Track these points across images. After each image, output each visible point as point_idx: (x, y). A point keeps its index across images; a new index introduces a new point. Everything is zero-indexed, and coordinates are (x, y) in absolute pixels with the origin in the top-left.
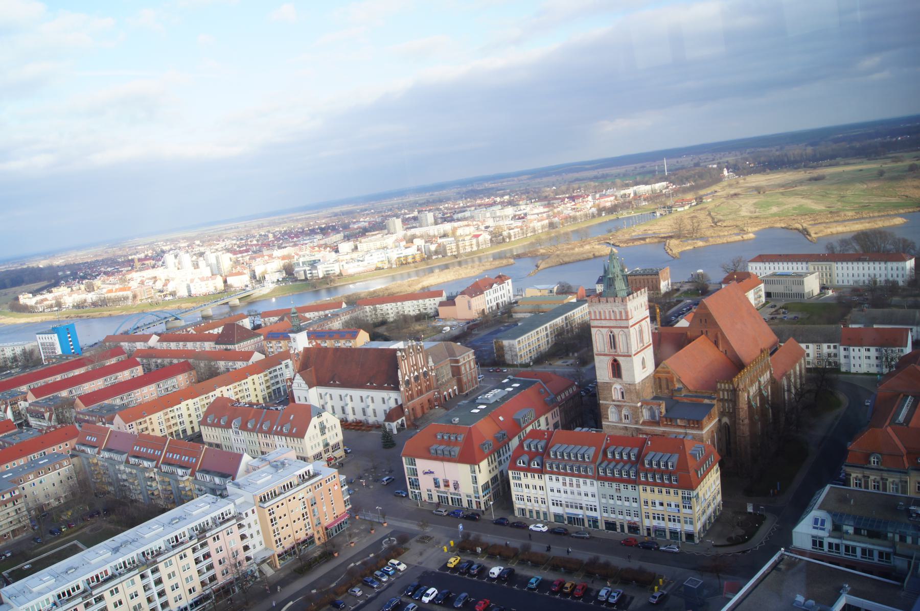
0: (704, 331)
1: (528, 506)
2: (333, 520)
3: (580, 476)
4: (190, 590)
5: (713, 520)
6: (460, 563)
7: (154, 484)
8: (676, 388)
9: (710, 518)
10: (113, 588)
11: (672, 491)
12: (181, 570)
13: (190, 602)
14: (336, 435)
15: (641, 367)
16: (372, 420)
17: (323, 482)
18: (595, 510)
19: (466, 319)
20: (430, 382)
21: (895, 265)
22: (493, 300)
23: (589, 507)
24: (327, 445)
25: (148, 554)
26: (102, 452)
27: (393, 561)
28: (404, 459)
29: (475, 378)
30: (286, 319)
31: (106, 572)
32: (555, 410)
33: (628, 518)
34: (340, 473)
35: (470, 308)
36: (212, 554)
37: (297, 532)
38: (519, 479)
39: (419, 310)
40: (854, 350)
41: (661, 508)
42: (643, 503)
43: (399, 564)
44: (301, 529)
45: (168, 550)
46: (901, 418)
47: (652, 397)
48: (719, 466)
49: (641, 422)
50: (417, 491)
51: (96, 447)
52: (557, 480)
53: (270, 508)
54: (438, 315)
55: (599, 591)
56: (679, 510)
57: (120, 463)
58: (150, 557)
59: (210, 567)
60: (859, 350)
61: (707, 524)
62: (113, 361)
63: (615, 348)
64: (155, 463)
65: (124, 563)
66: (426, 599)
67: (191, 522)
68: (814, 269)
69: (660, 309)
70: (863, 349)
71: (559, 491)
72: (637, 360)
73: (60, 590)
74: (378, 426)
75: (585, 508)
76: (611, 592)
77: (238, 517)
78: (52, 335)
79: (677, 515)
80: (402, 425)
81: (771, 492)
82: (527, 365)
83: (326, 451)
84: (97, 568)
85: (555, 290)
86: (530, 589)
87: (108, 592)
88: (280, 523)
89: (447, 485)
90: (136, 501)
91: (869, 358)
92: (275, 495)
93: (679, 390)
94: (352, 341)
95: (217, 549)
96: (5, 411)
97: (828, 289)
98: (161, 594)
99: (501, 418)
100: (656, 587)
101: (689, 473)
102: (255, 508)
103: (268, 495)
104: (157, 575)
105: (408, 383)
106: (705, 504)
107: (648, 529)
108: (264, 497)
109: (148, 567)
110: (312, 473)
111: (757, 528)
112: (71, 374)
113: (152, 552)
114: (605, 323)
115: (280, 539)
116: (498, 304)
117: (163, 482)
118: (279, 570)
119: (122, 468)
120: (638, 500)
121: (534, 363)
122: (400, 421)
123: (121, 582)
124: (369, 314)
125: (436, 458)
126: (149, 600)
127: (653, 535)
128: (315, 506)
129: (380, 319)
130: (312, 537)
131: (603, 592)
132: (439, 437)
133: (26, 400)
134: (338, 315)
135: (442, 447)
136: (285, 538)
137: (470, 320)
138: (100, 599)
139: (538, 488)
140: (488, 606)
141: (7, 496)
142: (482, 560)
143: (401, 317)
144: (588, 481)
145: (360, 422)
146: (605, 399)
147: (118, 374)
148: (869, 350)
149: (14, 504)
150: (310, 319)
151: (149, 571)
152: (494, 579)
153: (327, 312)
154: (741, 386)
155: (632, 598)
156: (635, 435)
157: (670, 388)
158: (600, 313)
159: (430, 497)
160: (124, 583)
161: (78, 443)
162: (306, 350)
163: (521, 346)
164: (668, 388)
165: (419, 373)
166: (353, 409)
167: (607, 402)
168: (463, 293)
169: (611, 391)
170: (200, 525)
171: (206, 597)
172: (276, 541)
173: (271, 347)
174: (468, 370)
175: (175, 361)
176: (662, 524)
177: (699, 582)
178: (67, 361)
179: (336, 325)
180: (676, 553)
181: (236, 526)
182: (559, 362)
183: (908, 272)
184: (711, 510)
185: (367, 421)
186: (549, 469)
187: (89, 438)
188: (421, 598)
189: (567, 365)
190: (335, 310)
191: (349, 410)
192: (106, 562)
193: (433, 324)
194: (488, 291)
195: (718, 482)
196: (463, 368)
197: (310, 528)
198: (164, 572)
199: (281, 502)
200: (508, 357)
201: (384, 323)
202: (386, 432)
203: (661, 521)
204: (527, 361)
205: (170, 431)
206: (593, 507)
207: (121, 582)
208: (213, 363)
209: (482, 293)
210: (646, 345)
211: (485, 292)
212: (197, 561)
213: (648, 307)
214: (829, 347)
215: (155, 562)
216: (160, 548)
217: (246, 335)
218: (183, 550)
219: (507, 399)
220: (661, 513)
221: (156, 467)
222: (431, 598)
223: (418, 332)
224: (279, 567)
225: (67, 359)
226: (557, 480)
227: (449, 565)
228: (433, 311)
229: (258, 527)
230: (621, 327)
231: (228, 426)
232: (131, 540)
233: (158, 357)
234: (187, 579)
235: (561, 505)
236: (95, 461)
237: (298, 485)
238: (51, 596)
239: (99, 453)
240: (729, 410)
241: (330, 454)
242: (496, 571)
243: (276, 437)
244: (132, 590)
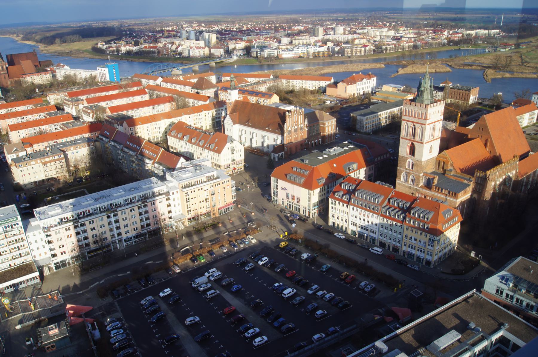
0: (480, 136)
1: (337, 222)
2: (224, 205)
3: (370, 211)
4: (134, 229)
5: (447, 256)
6: (287, 246)
7: (134, 165)
8: (449, 169)
9: (445, 254)
10: (91, 220)
11: (424, 233)
12: (131, 217)
13: (134, 235)
14: (240, 156)
15: (429, 151)
16: (265, 150)
17: (221, 183)
18: (375, 233)
19: (341, 98)
20: (304, 134)
22: (361, 89)
23: (372, 231)
24: (234, 160)
25: (114, 205)
26: (111, 142)
27: (249, 236)
28: (272, 178)
29: (334, 136)
31: (89, 210)
32: (372, 166)
33: (394, 243)
34: (232, 179)
35: (345, 91)
36: (149, 212)
37: (201, 208)
38: (335, 204)
39: (315, 87)
41: (415, 242)
42: (404, 236)
43: (252, 239)
44: (204, 207)
45: (124, 205)
47: (432, 171)
48: (461, 224)
49: (420, 186)
50: (276, 198)
51: (108, 138)
52: (357, 210)
53: (187, 192)
54: (326, 92)
55: (361, 282)
56: (425, 246)
57: (119, 149)
58: (114, 207)
59: (147, 219)
61: (442, 258)
62: (135, 89)
63: (414, 136)
64: (136, 153)
65: (99, 207)
66: (261, 263)
67: (140, 192)
69: (461, 114)
71: (356, 217)
72: (426, 147)
73: (62, 216)
74: (267, 154)
75: (369, 231)
76: (368, 285)
77: (167, 194)
79: (423, 248)
80: (282, 156)
81: (491, 247)
82: (368, 134)
83: (233, 164)
84: (86, 207)
85: (402, 89)
86: (322, 271)
87: (88, 222)
88: (192, 202)
89: (293, 199)
90: (125, 172)
92: (202, 182)
93: (451, 171)
94: (268, 100)
95: (152, 210)
96: (72, 109)
98: (118, 228)
99: (335, 165)
100: (396, 289)
101: (437, 225)
102: (179, 190)
103: (199, 181)
104: (116, 218)
105: (290, 132)
106: (443, 246)
107: (404, 252)
108: (185, 185)
109: (112, 212)
110: (215, 176)
111: (473, 268)
112: (110, 93)
113: (116, 205)
114: (411, 119)
115: (190, 210)
116: (364, 92)
117: (138, 165)
118: (187, 227)
119: (120, 152)
120: (402, 234)
121: (372, 134)
122: (280, 154)
123: (96, 218)
124: (285, 85)
125: (290, 182)
126: (111, 230)
127: (406, 256)
128: (213, 196)
129: (291, 89)
130: (210, 212)
131: (363, 284)
132: (294, 169)
133: (83, 104)
134: (265, 82)
135: (295, 176)
136: (193, 211)
137: (344, 98)
138: (83, 225)
139: (345, 212)
140: (294, 275)
141: (57, 157)
142: (298, 248)
143: (303, 90)
144: (375, 215)
145: (259, 150)
146: (401, 167)
147: (134, 97)
149: (60, 162)
150: (248, 82)
151: (112, 215)
152: (303, 260)
153: (261, 79)
154: (491, 177)
155: (379, 291)
156: (414, 192)
157: (445, 168)
158: (409, 112)
159: (283, 203)
160: (97, 219)
161: (99, 134)
162: (237, 101)
163: (368, 121)
164: (443, 168)
165: (298, 127)
166: (256, 141)
167: (402, 169)
168: (342, 81)
169: (406, 162)
170: (145, 194)
171: (144, 234)
172: (188, 211)
174: (330, 130)
175: (167, 95)
176: (413, 252)
177: (420, 293)
179: (263, 89)
180: (416, 271)
181: (165, 198)
182: (389, 136)
184: (447, 249)
185: (263, 150)
186: (352, 203)
187: (105, 132)
188: (258, 261)
189: (393, 139)
190: (263, 79)
191: (254, 141)
192: (90, 205)
193: (322, 97)
194: (359, 83)
195: (458, 234)
196: (327, 129)
197: (209, 207)
198: (120, 216)
199: (194, 190)
200: (358, 127)
201: (292, 92)
202: (270, 159)
203: (413, 250)
204: (369, 131)
205: (153, 135)
206: (374, 231)
207: (96, 218)
208: (187, 100)
209: (355, 83)
210: (435, 138)
211: (357, 83)
212: (140, 214)
213: (443, 114)
215: (116, 211)
216: (121, 203)
217: (210, 86)
218: (132, 207)
219: (343, 154)
220: (414, 245)
221: (136, 155)
222: (263, 263)
223: (311, 101)
224: (187, 225)
225: (111, 84)
226: (357, 210)
227: (280, 246)
228: (323, 89)
229: (180, 202)
230: (421, 124)
231: (182, 139)
232: (106, 196)
233: (158, 91)
234: (133, 223)
235: (356, 225)
236: (107, 146)
237: (205, 182)
238: (57, 219)
239: (109, 142)
240: (479, 190)
241: (235, 166)
242: (305, 256)
243: (206, 150)
244: (101, 223)
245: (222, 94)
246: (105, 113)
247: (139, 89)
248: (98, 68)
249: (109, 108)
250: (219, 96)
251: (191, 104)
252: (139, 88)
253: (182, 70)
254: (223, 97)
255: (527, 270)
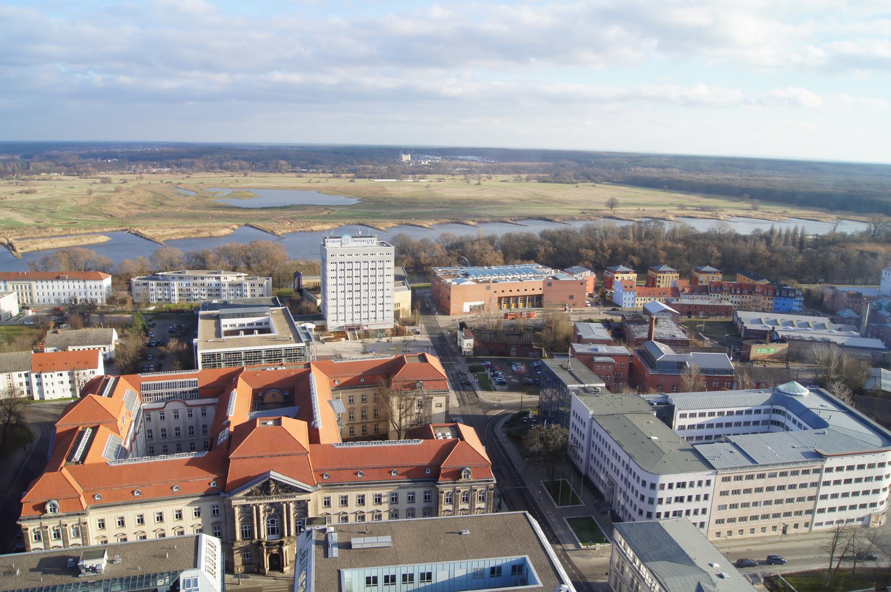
21: (93, 283)
40: (46, 376)
46: (78, 456)
60: (52, 376)
68: (13, 288)
70: (55, 374)
91: (62, 382)
97: (28, 308)
148: (61, 375)
183: (104, 290)
214: (20, 376)
255: (10, 572)
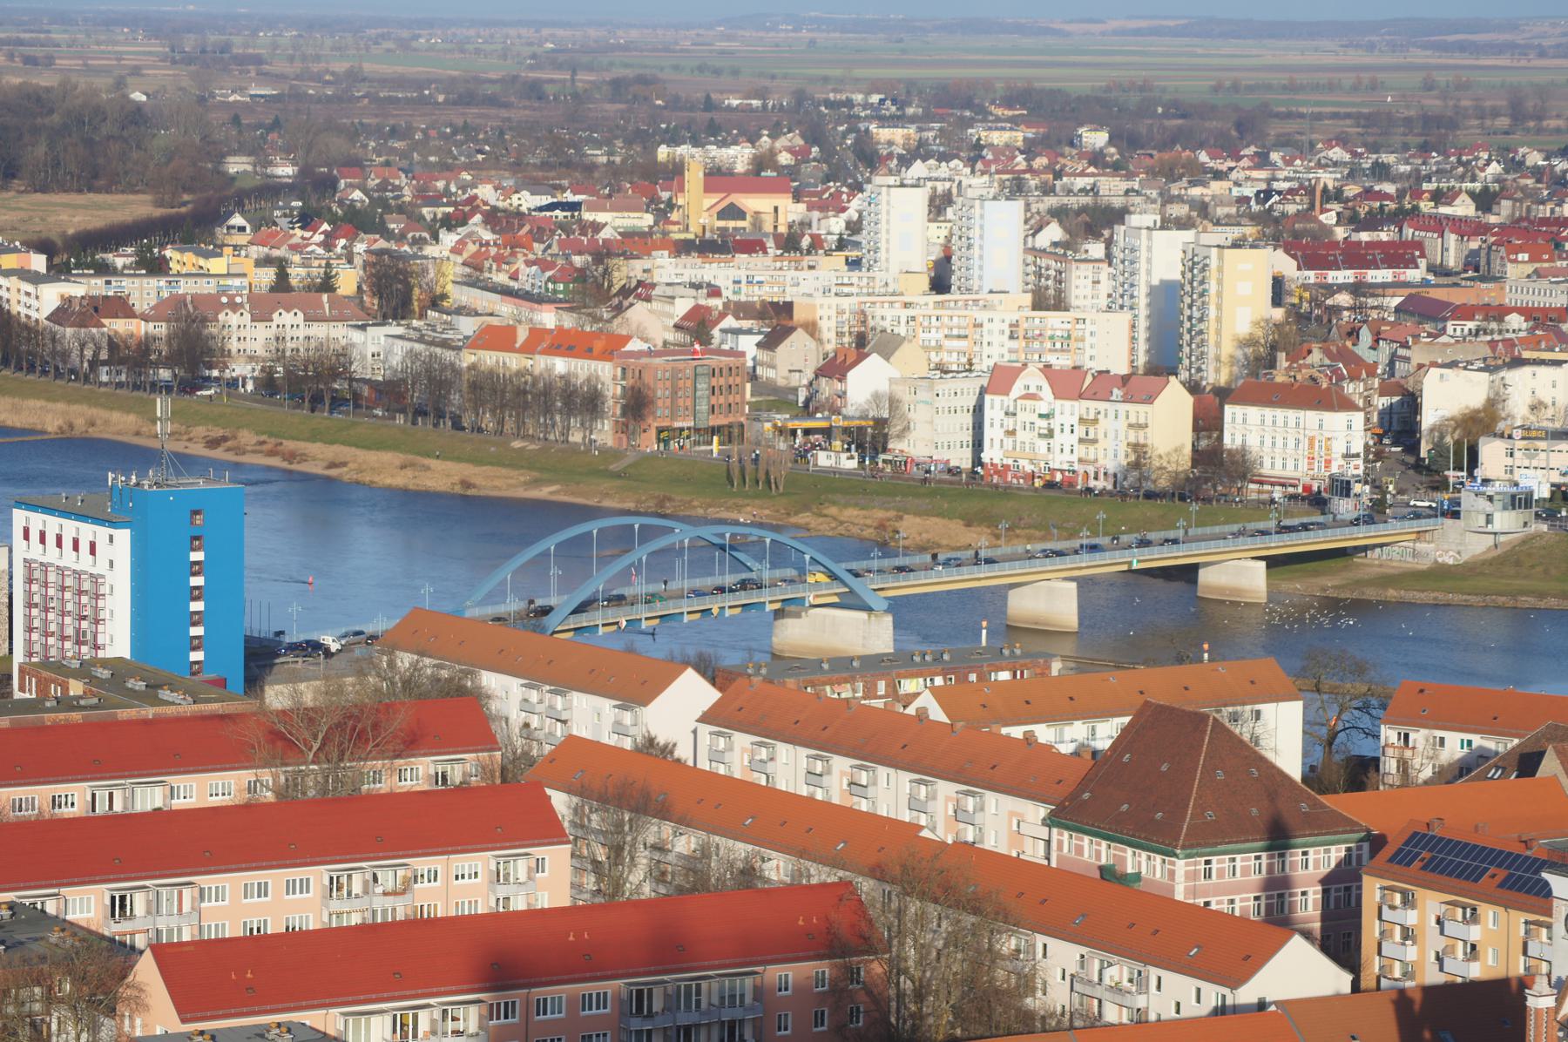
30: (1550, 765)
78: (102, 532)
112: (149, 797)
147: (422, 864)
173: (1407, 934)
175: (777, 868)
178: (150, 712)
208: (1007, 944)
225: (150, 695)
233: (684, 821)
245: (1411, 918)
246: (111, 1012)
247: (456, 774)
248: (19, 517)
249: (169, 956)
250: (1371, 929)
251: (1055, 996)
252: (462, 767)
253: (897, 607)
254: (1411, 953)
